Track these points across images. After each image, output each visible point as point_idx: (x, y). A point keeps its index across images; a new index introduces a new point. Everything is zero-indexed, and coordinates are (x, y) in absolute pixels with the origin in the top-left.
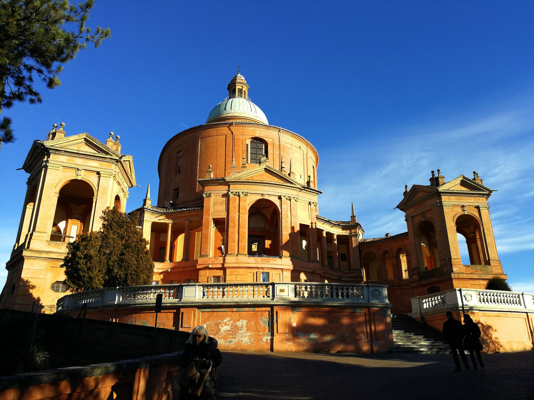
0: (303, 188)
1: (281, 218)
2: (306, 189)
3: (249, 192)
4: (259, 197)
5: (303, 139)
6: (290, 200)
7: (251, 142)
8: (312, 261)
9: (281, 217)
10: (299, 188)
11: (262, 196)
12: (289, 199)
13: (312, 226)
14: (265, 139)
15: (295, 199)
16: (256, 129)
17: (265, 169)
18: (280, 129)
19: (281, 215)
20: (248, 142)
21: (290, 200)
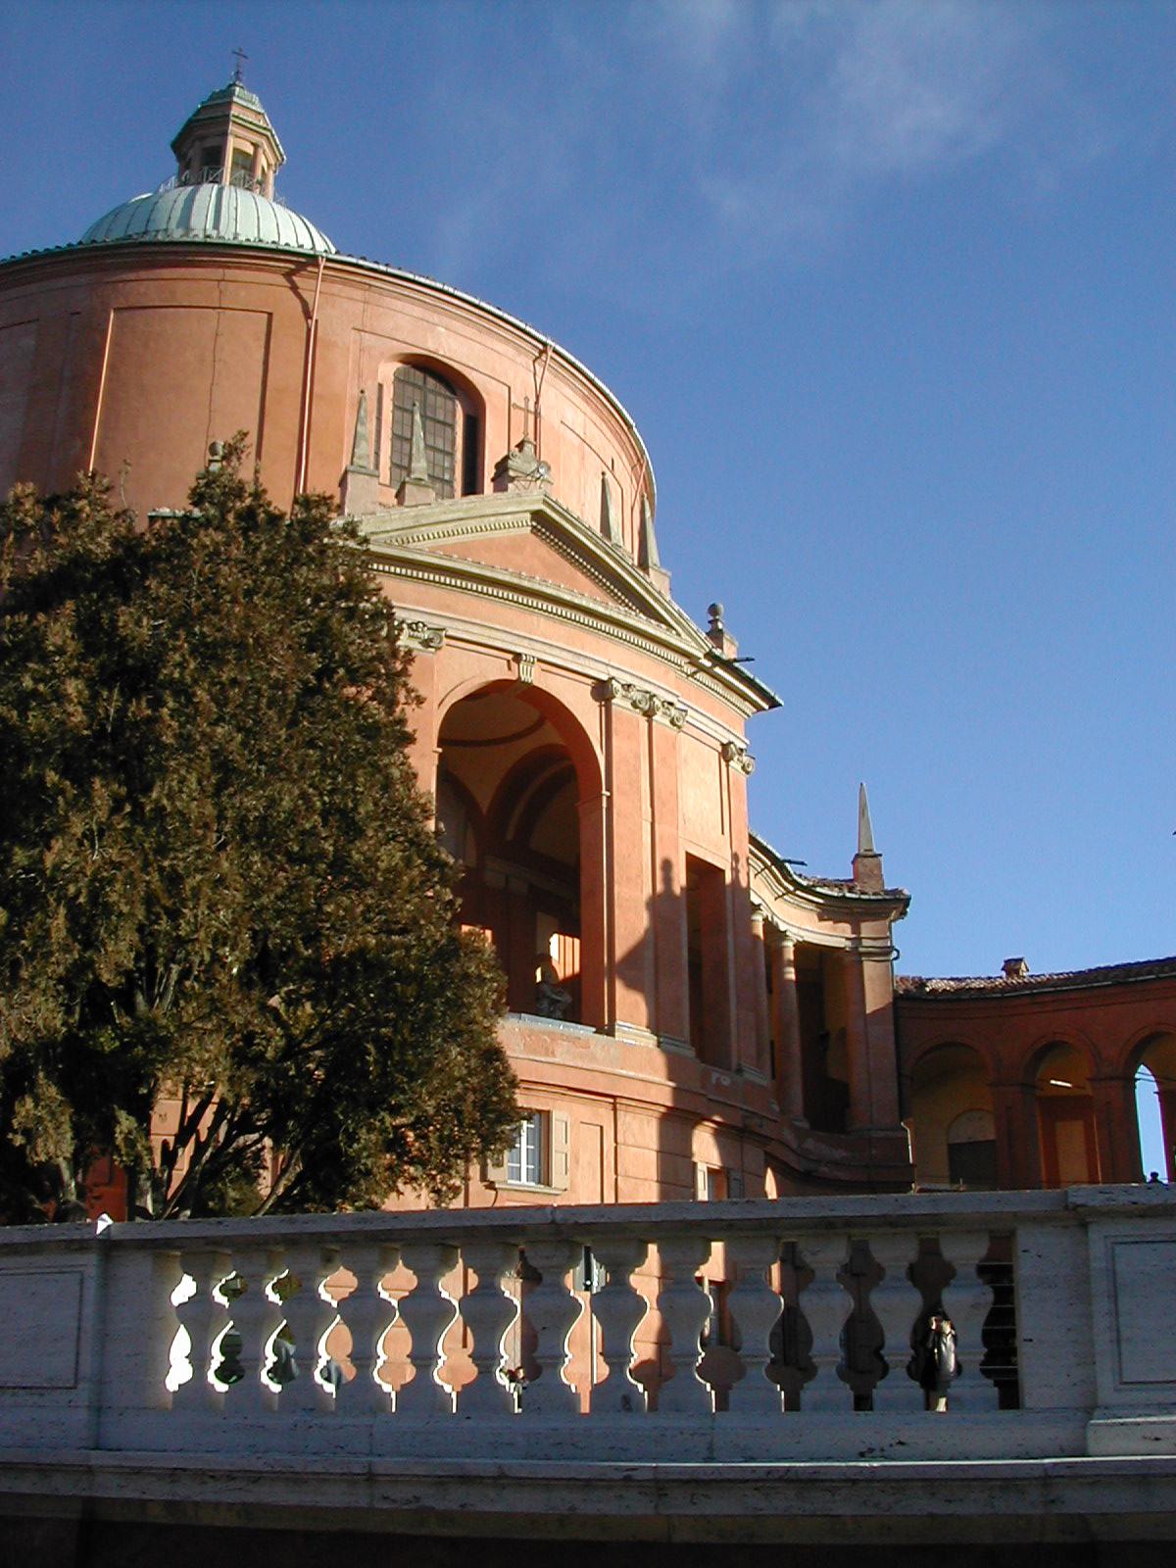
0: (708, 664)
1: (604, 805)
2: (717, 670)
3: (451, 633)
4: (496, 670)
5: (630, 427)
6: (649, 714)
7: (400, 380)
8: (734, 1066)
9: (604, 799)
10: (692, 660)
11: (514, 665)
12: (647, 707)
13: (735, 870)
14: (472, 376)
15: (673, 712)
16: (436, 318)
17: (538, 516)
18: (545, 344)
19: (609, 788)
20: (388, 371)
21: (649, 714)
